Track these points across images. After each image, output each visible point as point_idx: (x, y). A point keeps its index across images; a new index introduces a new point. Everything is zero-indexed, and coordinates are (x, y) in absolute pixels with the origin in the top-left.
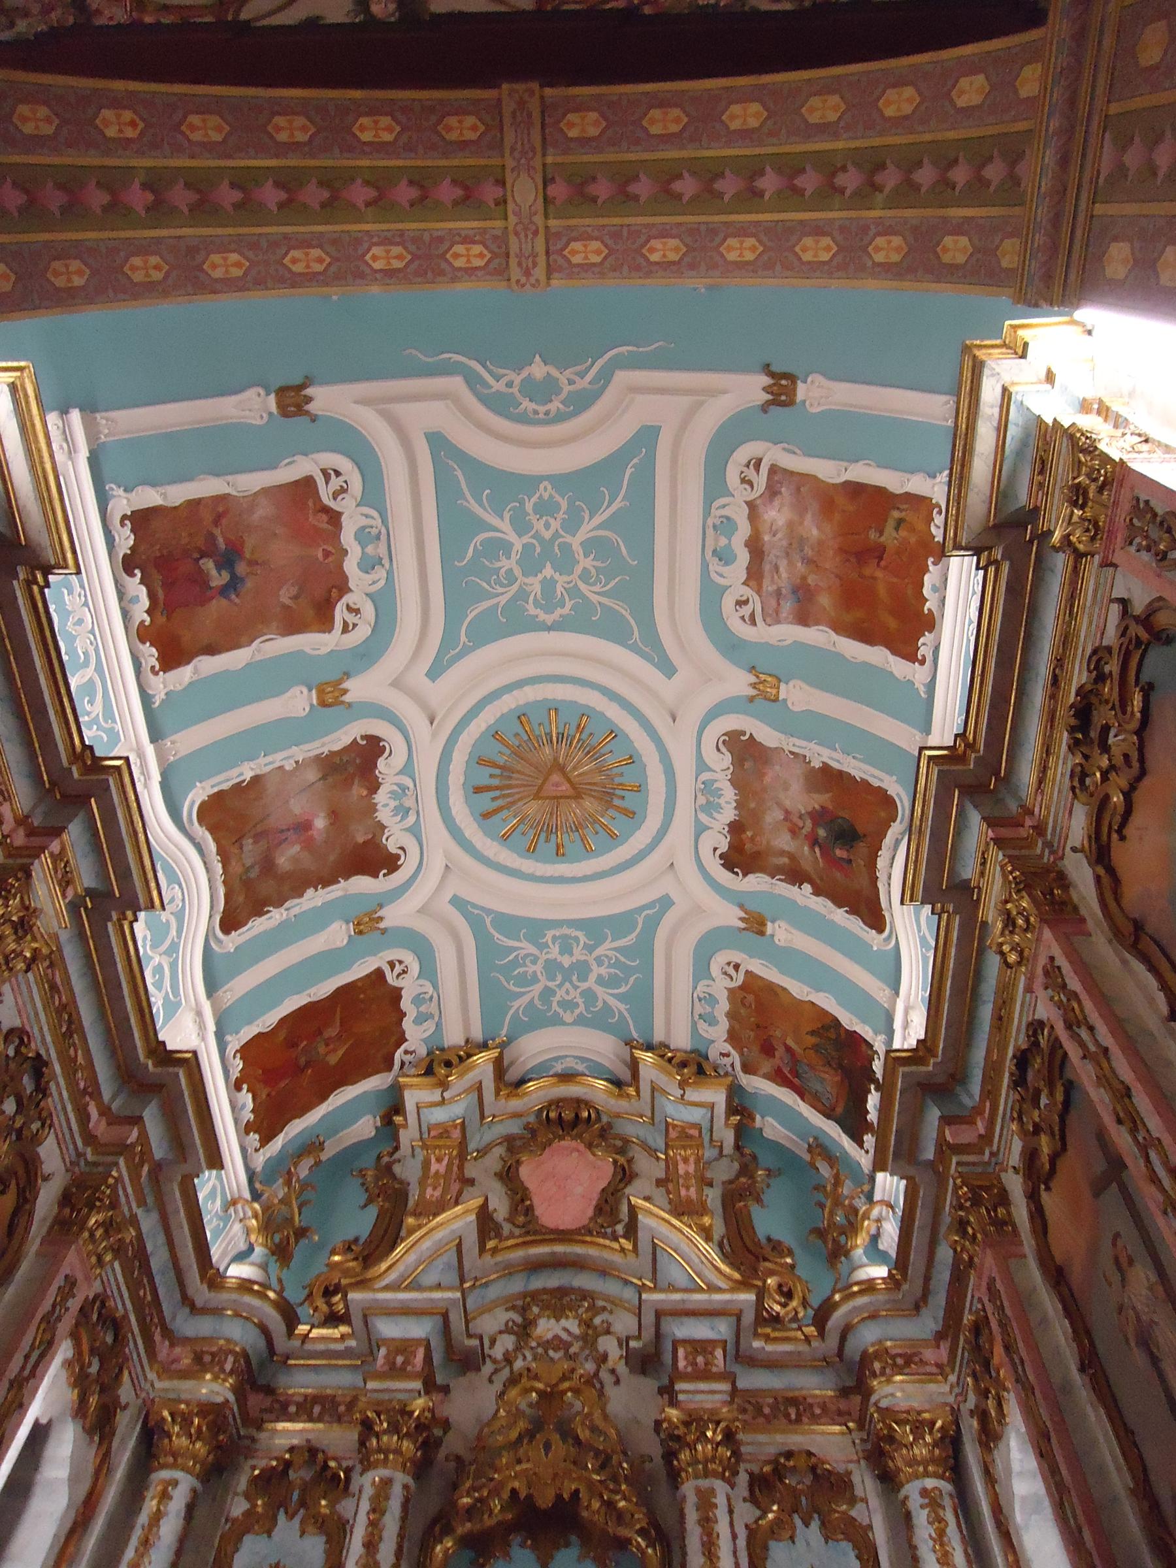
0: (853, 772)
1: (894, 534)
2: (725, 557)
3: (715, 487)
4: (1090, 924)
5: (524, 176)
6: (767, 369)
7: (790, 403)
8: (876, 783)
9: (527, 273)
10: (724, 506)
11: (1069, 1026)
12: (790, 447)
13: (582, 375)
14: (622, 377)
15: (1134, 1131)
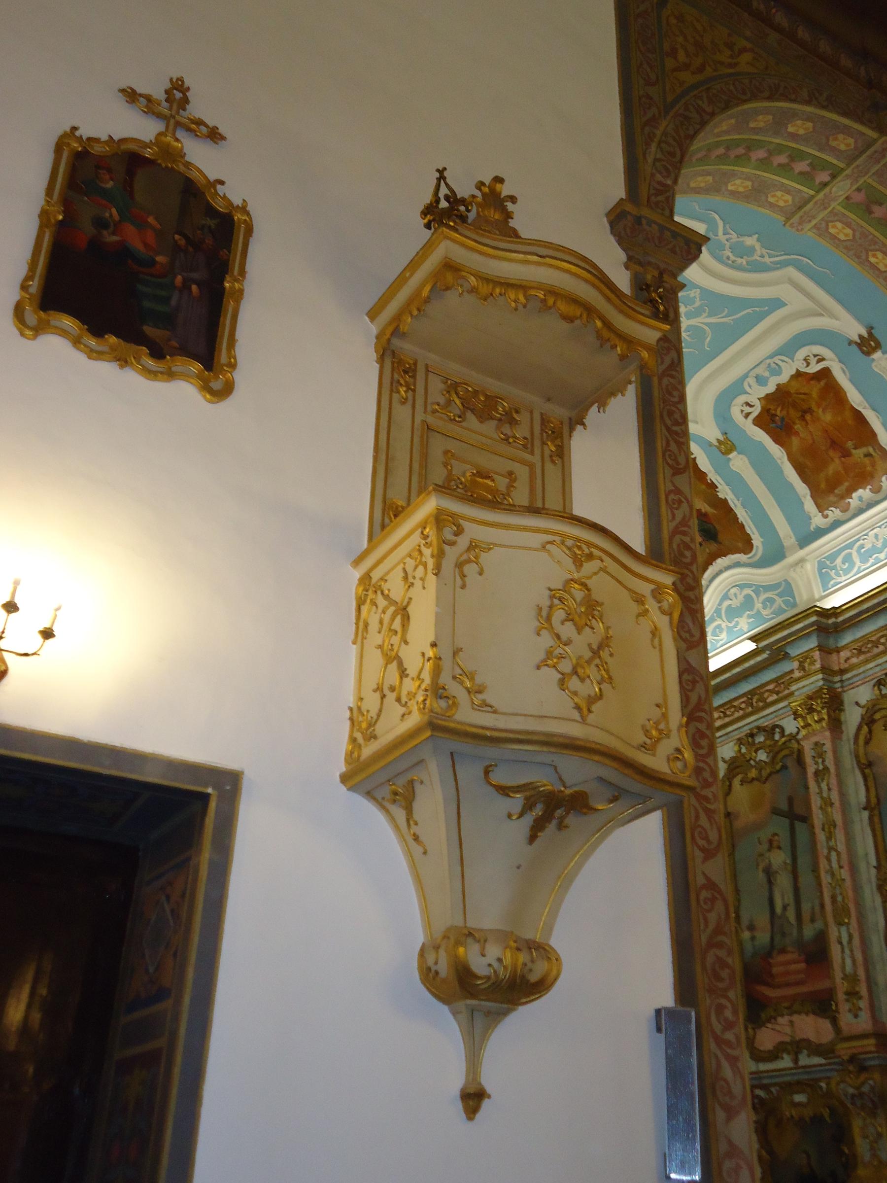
0: (739, 516)
1: (862, 456)
2: (761, 381)
3: (788, 350)
4: (844, 737)
5: (848, 182)
6: (870, 330)
7: (868, 354)
8: (748, 531)
9: (801, 223)
10: (783, 361)
11: (817, 773)
12: (845, 369)
13: (770, 256)
14: (791, 271)
15: (829, 838)
